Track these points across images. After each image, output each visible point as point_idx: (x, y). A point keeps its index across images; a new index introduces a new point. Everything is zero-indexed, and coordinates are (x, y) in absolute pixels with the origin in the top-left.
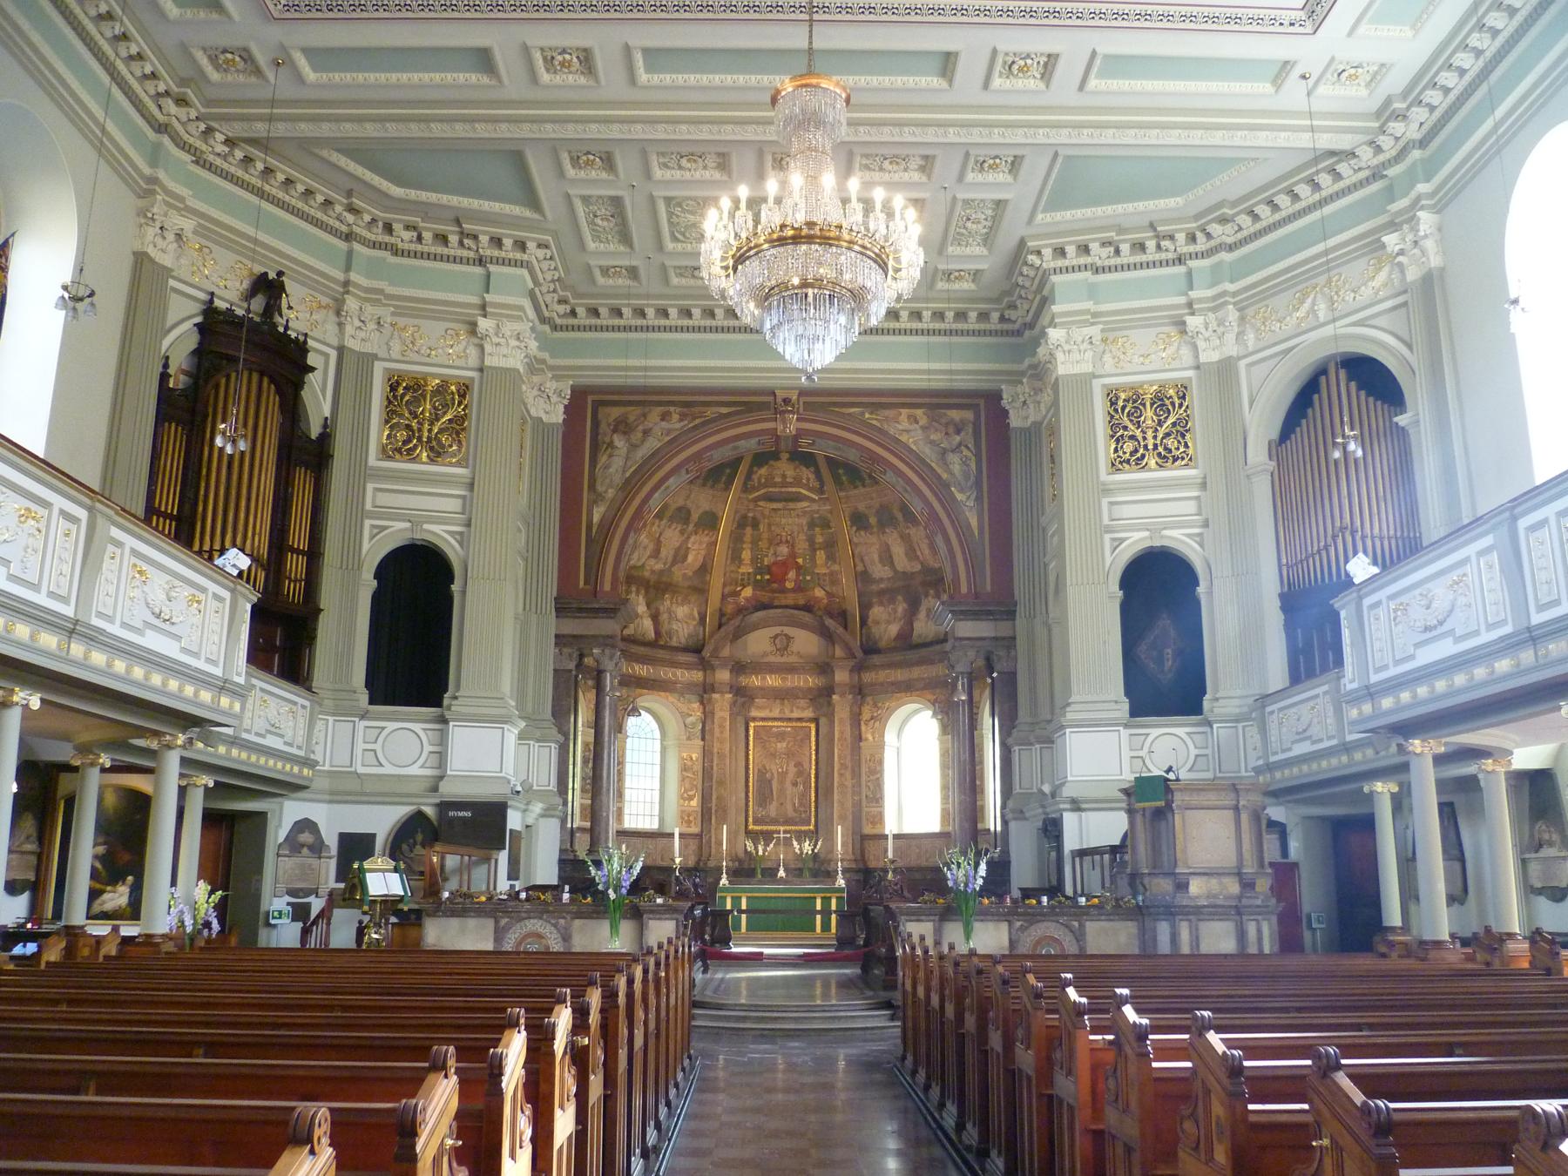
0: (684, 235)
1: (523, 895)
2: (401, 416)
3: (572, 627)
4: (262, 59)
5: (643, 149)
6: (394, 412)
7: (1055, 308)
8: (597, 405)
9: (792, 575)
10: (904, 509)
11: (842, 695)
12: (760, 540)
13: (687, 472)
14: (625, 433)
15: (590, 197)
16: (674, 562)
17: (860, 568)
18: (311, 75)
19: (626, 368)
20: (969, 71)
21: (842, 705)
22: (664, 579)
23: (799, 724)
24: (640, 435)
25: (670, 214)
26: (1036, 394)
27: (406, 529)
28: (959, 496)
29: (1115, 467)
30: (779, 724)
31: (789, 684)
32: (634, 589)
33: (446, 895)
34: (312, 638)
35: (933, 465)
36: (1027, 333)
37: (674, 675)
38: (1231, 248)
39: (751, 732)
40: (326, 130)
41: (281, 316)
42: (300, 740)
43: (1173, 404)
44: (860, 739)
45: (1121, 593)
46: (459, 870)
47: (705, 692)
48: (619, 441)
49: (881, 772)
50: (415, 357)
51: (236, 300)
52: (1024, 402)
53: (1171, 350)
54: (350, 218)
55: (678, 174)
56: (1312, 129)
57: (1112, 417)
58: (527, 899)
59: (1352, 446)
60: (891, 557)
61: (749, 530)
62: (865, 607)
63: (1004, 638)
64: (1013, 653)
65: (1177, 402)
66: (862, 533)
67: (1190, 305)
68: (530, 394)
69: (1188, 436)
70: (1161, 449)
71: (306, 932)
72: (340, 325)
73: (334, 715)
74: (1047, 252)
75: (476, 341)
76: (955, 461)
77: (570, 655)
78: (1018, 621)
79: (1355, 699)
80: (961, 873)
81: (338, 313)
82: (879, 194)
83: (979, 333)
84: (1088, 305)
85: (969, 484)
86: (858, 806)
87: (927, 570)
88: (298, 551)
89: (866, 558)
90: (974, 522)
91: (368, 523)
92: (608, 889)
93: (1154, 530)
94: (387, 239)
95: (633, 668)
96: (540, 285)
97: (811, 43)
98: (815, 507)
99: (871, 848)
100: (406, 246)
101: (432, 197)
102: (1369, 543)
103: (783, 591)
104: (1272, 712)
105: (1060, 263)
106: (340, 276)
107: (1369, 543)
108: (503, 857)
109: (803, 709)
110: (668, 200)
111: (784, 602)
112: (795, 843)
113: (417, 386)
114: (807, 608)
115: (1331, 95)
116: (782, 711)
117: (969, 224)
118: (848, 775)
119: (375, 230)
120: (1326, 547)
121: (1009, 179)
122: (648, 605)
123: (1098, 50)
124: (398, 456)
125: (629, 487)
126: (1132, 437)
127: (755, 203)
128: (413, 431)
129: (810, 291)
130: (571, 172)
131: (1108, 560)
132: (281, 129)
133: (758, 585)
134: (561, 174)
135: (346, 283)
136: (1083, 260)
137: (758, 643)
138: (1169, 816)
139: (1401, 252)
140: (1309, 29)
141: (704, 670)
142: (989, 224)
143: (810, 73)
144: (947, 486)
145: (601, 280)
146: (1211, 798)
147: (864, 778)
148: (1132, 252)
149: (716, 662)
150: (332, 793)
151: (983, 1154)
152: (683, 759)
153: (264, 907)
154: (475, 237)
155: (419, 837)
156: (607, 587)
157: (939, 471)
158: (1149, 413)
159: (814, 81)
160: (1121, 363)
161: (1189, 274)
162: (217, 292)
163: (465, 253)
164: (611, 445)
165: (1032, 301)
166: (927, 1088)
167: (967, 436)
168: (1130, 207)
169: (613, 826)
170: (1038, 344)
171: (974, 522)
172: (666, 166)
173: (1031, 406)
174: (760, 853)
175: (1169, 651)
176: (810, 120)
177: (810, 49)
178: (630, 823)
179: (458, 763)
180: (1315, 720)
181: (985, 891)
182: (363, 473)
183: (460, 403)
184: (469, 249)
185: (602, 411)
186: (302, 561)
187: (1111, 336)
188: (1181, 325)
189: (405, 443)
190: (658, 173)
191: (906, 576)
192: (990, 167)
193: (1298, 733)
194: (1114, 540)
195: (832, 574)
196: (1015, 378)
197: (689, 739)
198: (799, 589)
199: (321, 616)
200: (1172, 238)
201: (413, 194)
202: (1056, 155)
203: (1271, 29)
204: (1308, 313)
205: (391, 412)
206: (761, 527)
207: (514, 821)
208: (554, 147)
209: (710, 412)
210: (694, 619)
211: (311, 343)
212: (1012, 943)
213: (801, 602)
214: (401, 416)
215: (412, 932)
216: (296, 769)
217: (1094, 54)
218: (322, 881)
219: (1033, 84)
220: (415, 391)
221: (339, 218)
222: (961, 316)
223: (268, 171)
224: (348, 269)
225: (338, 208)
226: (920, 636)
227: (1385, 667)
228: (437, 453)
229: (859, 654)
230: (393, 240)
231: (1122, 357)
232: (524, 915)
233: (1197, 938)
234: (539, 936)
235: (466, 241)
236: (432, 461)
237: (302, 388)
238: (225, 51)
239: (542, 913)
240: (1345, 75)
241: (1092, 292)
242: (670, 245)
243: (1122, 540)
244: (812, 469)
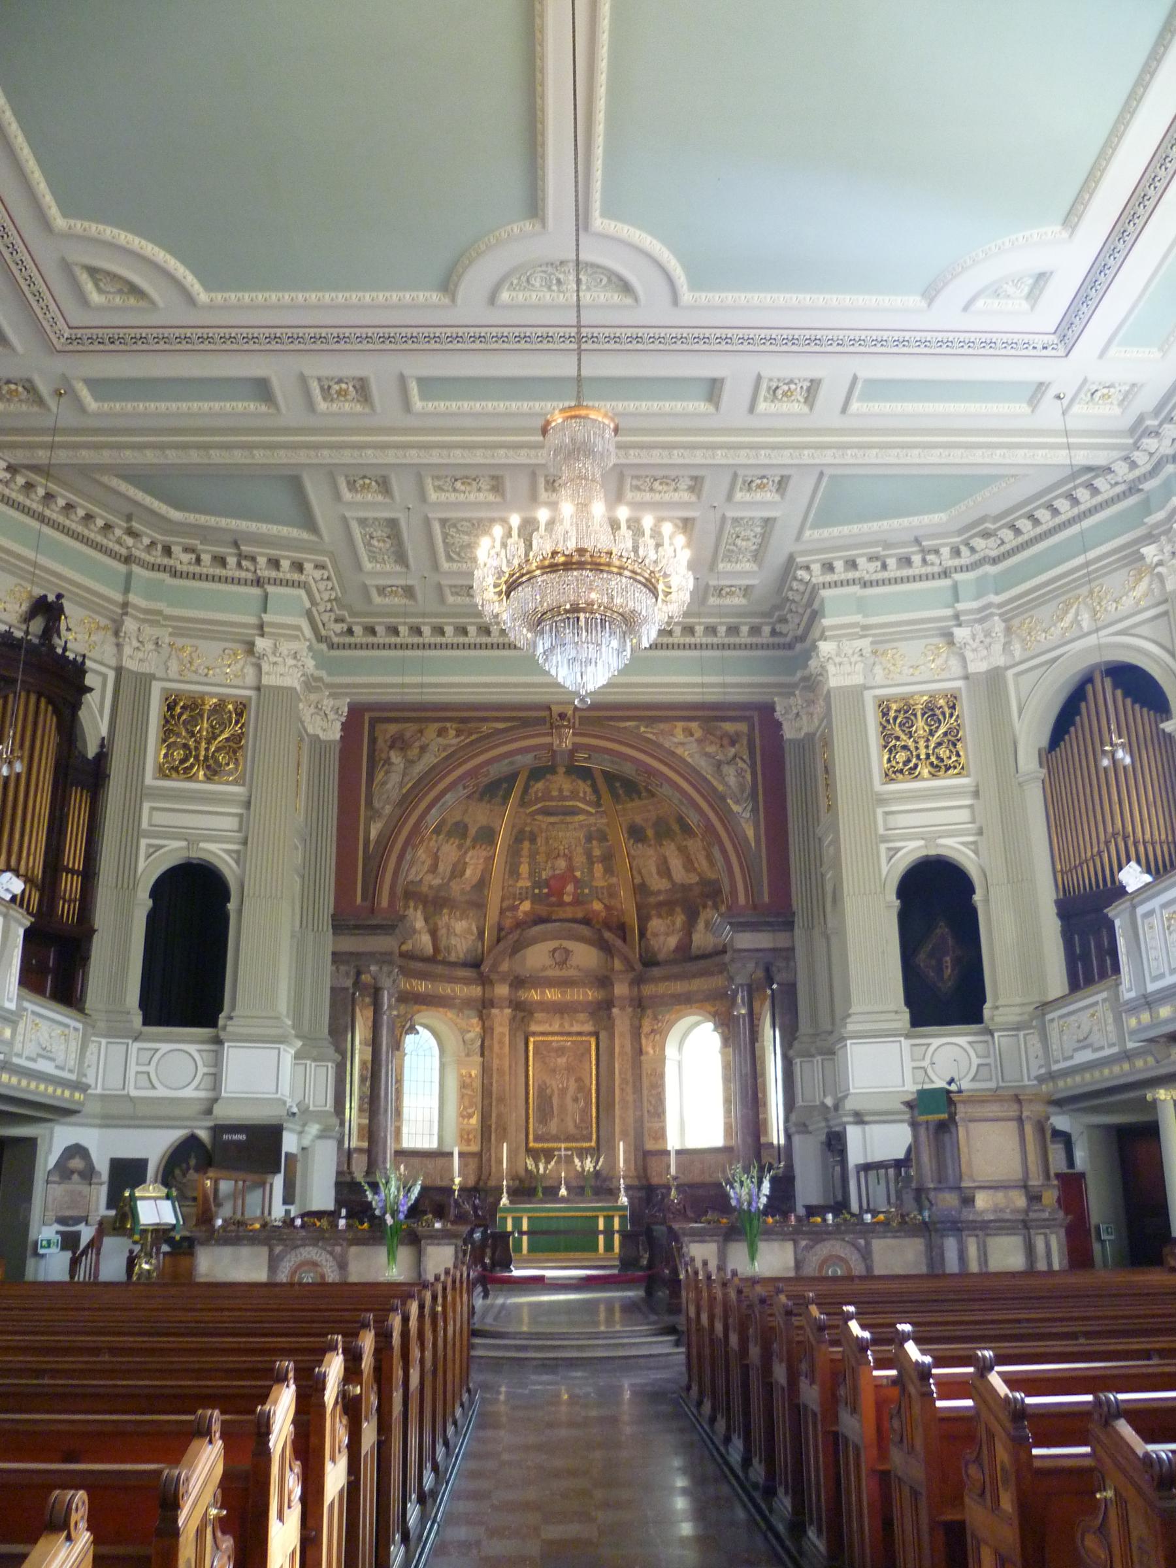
0: (458, 554)
1: (298, 1222)
2: (178, 735)
3: (349, 944)
4: (44, 389)
5: (418, 473)
6: (170, 731)
7: (826, 622)
8: (374, 722)
9: (570, 888)
10: (680, 820)
11: (622, 1008)
12: (538, 853)
13: (464, 788)
14: (402, 749)
15: (366, 519)
17: (638, 880)
18: (92, 405)
19: (403, 685)
20: (735, 396)
21: (621, 1019)
22: (442, 894)
23: (579, 1038)
24: (416, 751)
25: (445, 535)
26: (808, 705)
27: (181, 848)
28: (736, 808)
29: (889, 776)
30: (560, 1038)
31: (568, 997)
32: (412, 904)
33: (219, 1222)
34: (85, 959)
35: (709, 777)
36: (799, 647)
37: (453, 990)
38: (995, 561)
39: (531, 1047)
40: (106, 457)
41: (59, 637)
42: (71, 1063)
43: (944, 714)
44: (641, 1052)
45: (897, 903)
46: (234, 1196)
47: (484, 1007)
48: (396, 758)
49: (662, 1086)
50: (195, 678)
51: (15, 622)
52: (798, 714)
53: (939, 661)
54: (130, 541)
55: (452, 497)
56: (1069, 447)
57: (884, 727)
58: (303, 1226)
59: (1120, 754)
60: (668, 869)
61: (526, 844)
62: (643, 920)
63: (781, 950)
64: (792, 964)
65: (948, 712)
66: (640, 845)
67: (957, 617)
68: (306, 711)
69: (959, 745)
70: (933, 759)
71: (75, 1263)
72: (119, 646)
73: (106, 1036)
74: (816, 568)
75: (254, 660)
76: (730, 773)
77: (347, 974)
78: (797, 931)
79: (1133, 1008)
80: (744, 1192)
81: (116, 633)
82: (648, 521)
83: (751, 647)
84: (858, 618)
85: (745, 795)
86: (640, 1122)
87: (704, 882)
88: (73, 872)
89: (643, 871)
90: (750, 833)
91: (143, 842)
92: (385, 1214)
93: (929, 839)
94: (166, 561)
95: (411, 985)
96: (318, 604)
97: (579, 369)
98: (592, 820)
99: (654, 1164)
100: (185, 568)
101: (212, 521)
102: (1141, 849)
103: (561, 904)
104: (1052, 1020)
105: (829, 578)
106: (119, 598)
107: (1141, 849)
108: (278, 1181)
109: (583, 1023)
110: (443, 522)
111: (562, 915)
112: (577, 1161)
113: (194, 706)
114: (586, 921)
115: (1085, 414)
116: (561, 1025)
117: (739, 542)
118: (629, 1089)
119: (154, 553)
120: (1100, 853)
121: (777, 498)
122: (426, 920)
123: (859, 375)
124: (174, 775)
125: (406, 802)
126: (905, 748)
127: (528, 528)
128: (189, 749)
129: (582, 616)
130: (347, 495)
131: (885, 869)
132: (62, 456)
133: (536, 899)
134: (338, 497)
135: (125, 605)
136: (851, 575)
137: (537, 957)
138: (953, 1130)
139: (1160, 563)
140: (1061, 352)
141: (483, 985)
142: (758, 540)
143: (579, 406)
144: (723, 798)
145: (377, 600)
146: (994, 1109)
147: (645, 1092)
148: (899, 567)
149: (494, 977)
150: (105, 1117)
151: (769, 1492)
152: (462, 1075)
153: (32, 1236)
154: (253, 559)
155: (193, 1162)
156: (385, 903)
157: (715, 783)
158: (920, 723)
159: (583, 412)
160: (891, 676)
161: (955, 587)
163: (243, 574)
164: (388, 761)
165: (802, 615)
166: (712, 1420)
167: (742, 748)
168: (895, 523)
169: (391, 1146)
170: (809, 658)
171: (750, 833)
172: (439, 489)
173: (804, 718)
174: (541, 1171)
175: (948, 959)
176: (579, 450)
177: (579, 375)
178: (407, 1143)
179: (232, 1086)
180: (1096, 1028)
181: (770, 1209)
182: (139, 793)
183: (237, 722)
184: (247, 570)
185: (380, 727)
186: (77, 881)
187: (881, 648)
188: (949, 638)
189: (182, 761)
190: (433, 496)
191: (685, 888)
192: (758, 486)
193: (1079, 1041)
194: (889, 849)
195: (610, 886)
196: (787, 690)
197: (468, 1055)
198: (577, 901)
199: (96, 937)
200: (937, 552)
201: (191, 518)
202: (822, 474)
203: (1025, 352)
204: (1072, 623)
205: (167, 732)
206: (539, 840)
207: (290, 1143)
208: (331, 472)
209: (485, 728)
210: (472, 934)
211: (88, 663)
212: (798, 1265)
213: (580, 915)
214: (178, 735)
215: (184, 1262)
216: (67, 1093)
217: (855, 379)
218: (93, 1206)
219: (796, 407)
220: (192, 710)
221: (119, 542)
222: (733, 630)
223: (49, 497)
224: (127, 590)
225: (118, 532)
226: (699, 948)
227: (1162, 976)
228: (213, 771)
229: (638, 966)
230: (172, 562)
231: (892, 668)
232: (299, 1242)
233: (985, 1254)
234: (315, 1264)
235: (244, 563)
236: (208, 779)
237: (80, 709)
238: (8, 382)
239: (318, 1240)
240: (1098, 394)
241: (861, 606)
242: (445, 565)
243: (898, 850)
244: (589, 782)
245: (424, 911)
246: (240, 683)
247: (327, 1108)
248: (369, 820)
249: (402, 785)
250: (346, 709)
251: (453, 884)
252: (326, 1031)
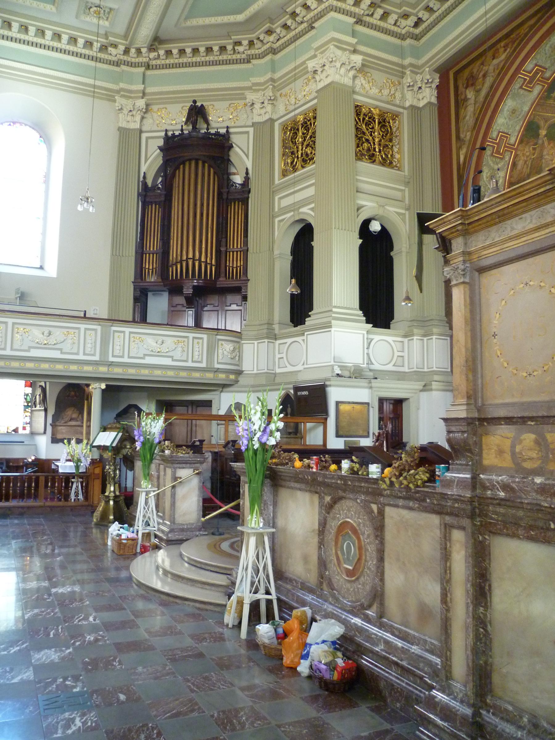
24: (480, 80)
48: (470, 94)
73: (257, 339)
119: (256, 46)
125: (478, 121)
150: (253, 386)
162: (168, 128)
164: (466, 99)
189: (292, 163)
199: (249, 284)
211: (231, 130)
230: (268, 46)
248: (459, 149)
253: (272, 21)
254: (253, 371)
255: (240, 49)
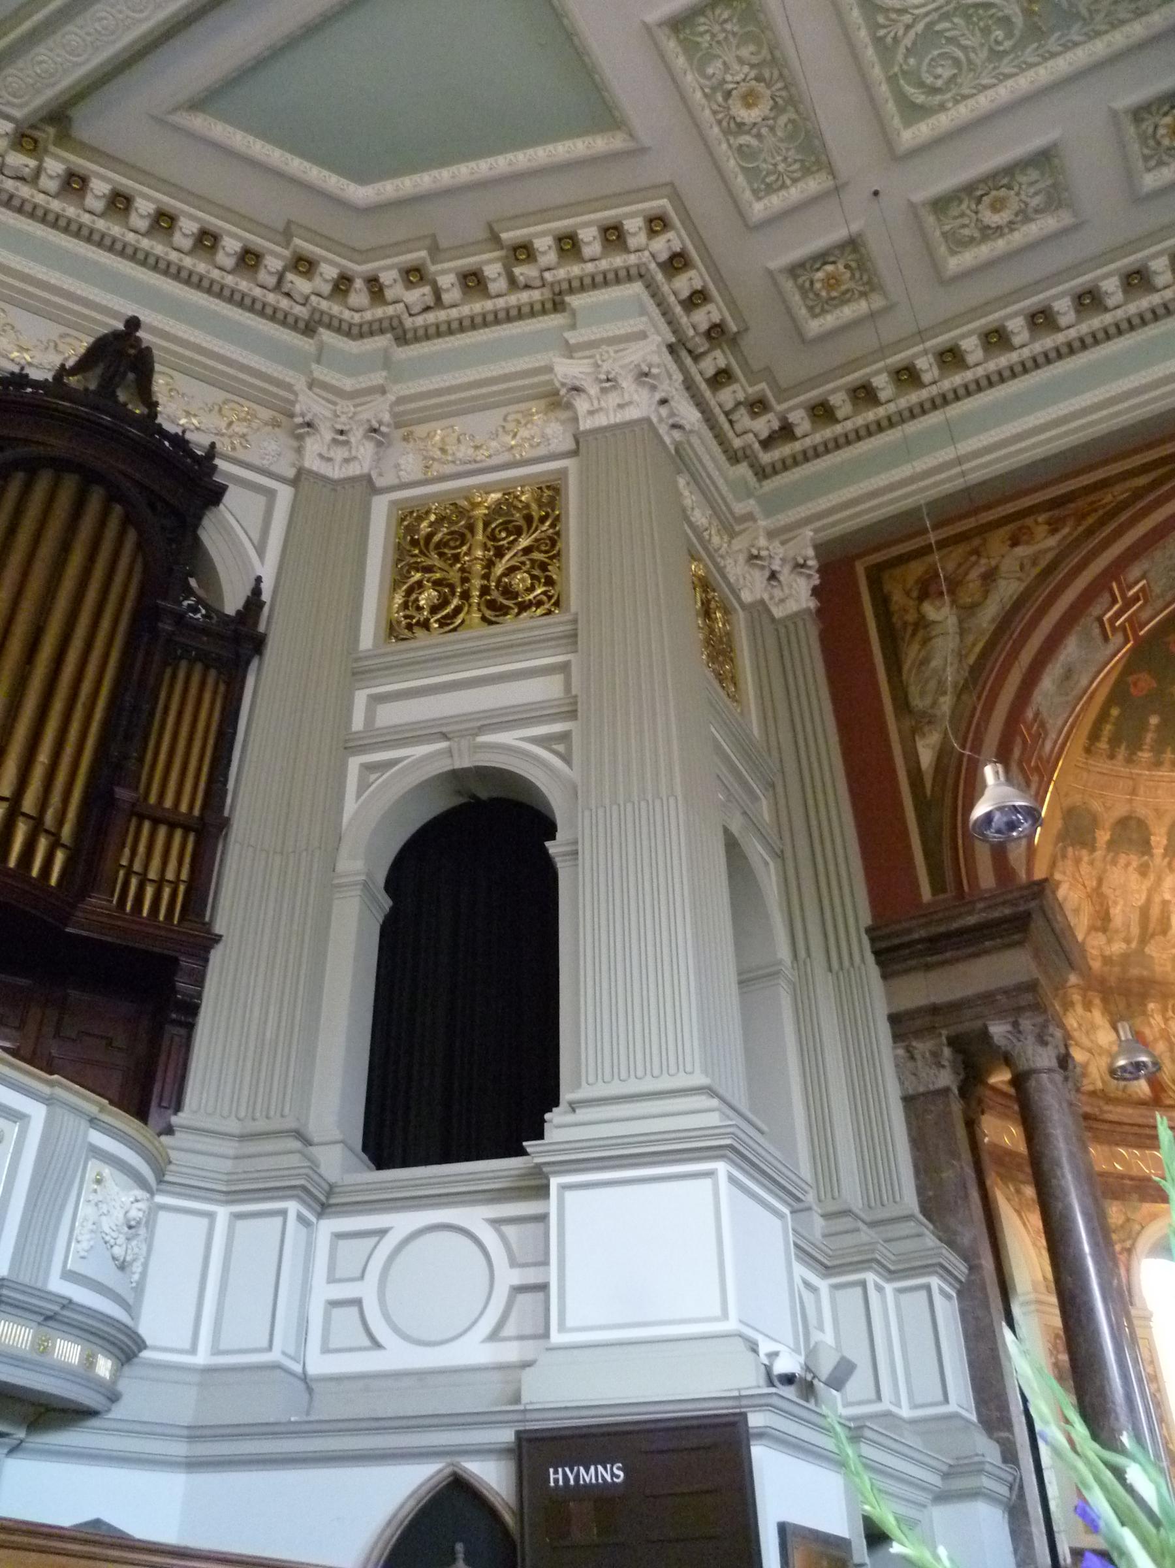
8: (876, 576)
16: (1144, 940)
22: (1135, 972)
73: (231, 1196)
77: (936, 1055)
150: (196, 1433)
156: (987, 879)
164: (922, 623)
199: (216, 956)
201: (389, 189)
230: (390, 310)
245: (1106, 1010)
246: (542, 451)
247: (952, 1407)
249: (961, 656)
250: (811, 552)
251: (1151, 950)
252: (910, 1200)
253: (435, 251)
254: (193, 1350)
255: (301, 285)
